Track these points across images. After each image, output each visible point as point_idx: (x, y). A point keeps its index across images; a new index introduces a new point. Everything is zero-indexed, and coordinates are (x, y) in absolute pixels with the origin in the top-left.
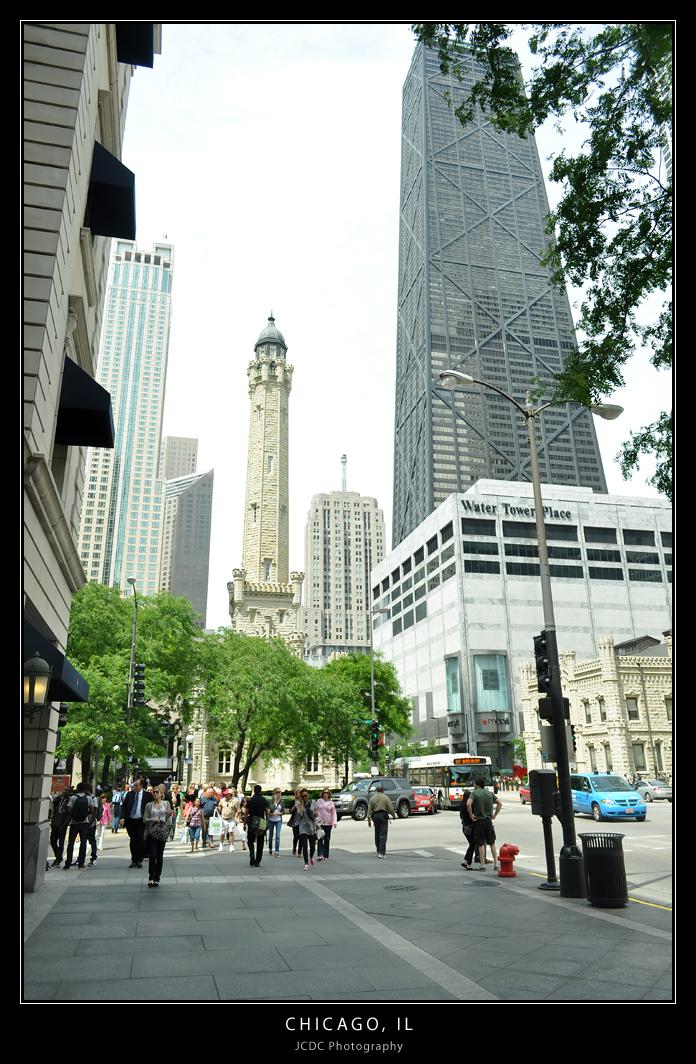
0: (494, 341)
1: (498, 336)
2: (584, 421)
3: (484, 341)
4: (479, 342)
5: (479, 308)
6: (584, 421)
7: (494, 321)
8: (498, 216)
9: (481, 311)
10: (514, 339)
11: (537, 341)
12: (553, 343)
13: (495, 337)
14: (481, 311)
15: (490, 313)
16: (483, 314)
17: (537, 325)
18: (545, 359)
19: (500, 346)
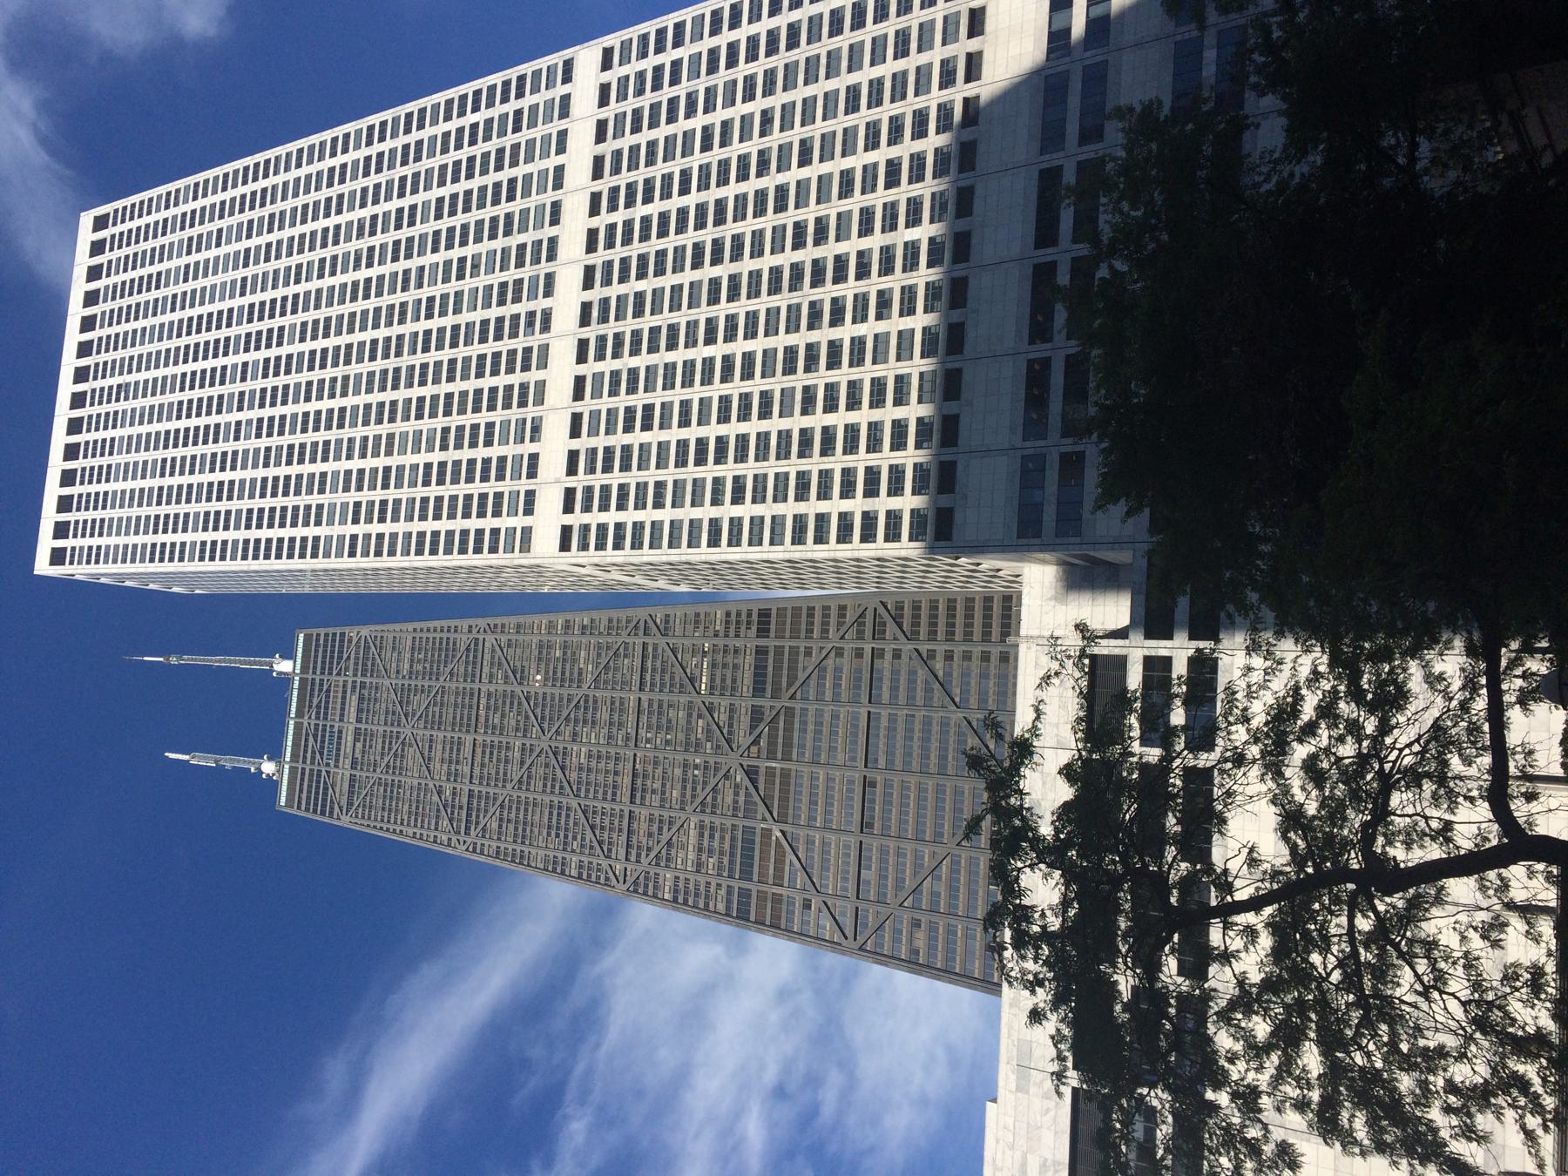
0: (761, 786)
1: (751, 773)
2: (907, 612)
3: (761, 808)
4: (764, 819)
5: (702, 803)
6: (907, 612)
7: (726, 776)
8: (546, 726)
9: (709, 799)
10: (756, 742)
11: (758, 690)
12: (761, 652)
13: (754, 782)
14: (709, 799)
15: (713, 782)
16: (714, 799)
17: (729, 682)
18: (790, 685)
19: (770, 772)
